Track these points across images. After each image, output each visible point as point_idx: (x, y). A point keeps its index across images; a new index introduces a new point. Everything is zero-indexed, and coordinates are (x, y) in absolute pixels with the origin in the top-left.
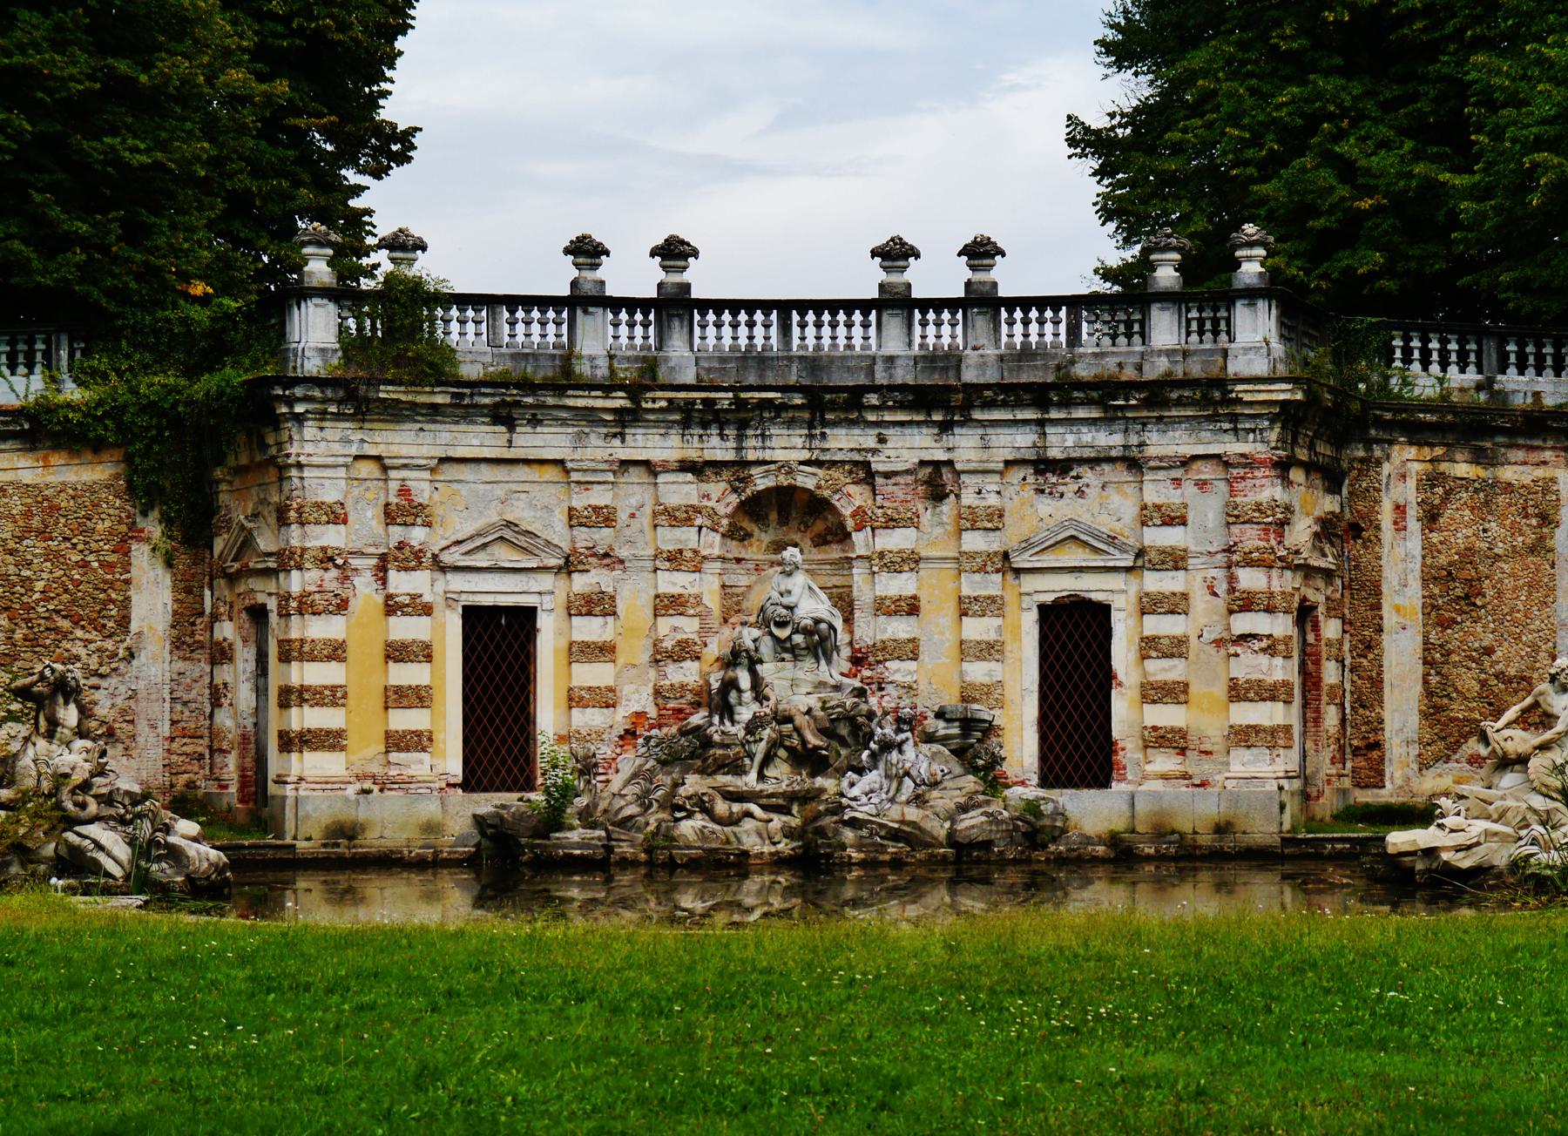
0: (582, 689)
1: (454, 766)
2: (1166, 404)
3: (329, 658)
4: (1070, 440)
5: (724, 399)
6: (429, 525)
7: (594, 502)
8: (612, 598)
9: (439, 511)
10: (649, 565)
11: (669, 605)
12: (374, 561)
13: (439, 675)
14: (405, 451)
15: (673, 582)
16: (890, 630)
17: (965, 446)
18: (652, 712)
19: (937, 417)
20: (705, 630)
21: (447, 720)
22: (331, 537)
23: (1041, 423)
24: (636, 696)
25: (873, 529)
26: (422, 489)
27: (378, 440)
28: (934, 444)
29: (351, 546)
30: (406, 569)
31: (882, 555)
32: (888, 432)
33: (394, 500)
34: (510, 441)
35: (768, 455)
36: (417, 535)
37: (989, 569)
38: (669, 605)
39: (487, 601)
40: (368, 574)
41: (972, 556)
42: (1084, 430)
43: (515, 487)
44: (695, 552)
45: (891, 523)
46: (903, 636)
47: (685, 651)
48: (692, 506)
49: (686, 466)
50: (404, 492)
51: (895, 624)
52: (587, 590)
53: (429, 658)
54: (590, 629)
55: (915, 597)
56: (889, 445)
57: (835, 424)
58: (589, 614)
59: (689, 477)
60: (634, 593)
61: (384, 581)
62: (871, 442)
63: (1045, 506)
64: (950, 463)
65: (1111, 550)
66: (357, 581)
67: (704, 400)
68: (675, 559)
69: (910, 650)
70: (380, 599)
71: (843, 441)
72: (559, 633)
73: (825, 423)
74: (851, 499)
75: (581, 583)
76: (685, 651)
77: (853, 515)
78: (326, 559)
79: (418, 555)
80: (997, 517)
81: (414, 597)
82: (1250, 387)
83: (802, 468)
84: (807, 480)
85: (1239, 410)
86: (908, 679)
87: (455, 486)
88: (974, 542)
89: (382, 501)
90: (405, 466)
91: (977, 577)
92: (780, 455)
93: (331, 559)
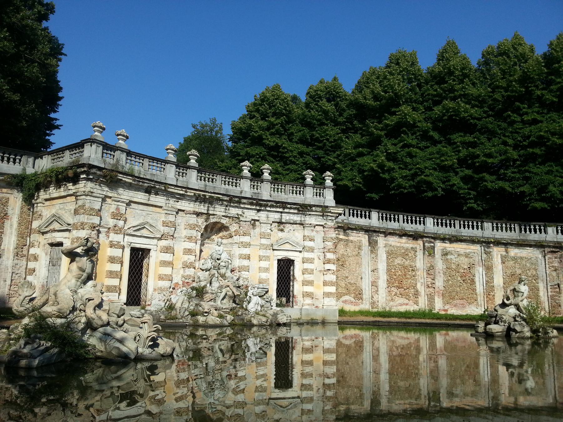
17: (262, 216)
18: (181, 283)
30: (117, 233)
36: (121, 223)
39: (138, 246)
41: (263, 245)
42: (291, 215)
45: (244, 234)
46: (246, 265)
50: (118, 209)
52: (166, 245)
59: (195, 216)
62: (240, 213)
63: (280, 234)
64: (258, 221)
68: (190, 238)
69: (247, 269)
70: (107, 242)
71: (234, 211)
73: (230, 206)
74: (234, 228)
77: (235, 231)
84: (224, 221)
85: (329, 214)
88: (264, 241)
92: (218, 213)
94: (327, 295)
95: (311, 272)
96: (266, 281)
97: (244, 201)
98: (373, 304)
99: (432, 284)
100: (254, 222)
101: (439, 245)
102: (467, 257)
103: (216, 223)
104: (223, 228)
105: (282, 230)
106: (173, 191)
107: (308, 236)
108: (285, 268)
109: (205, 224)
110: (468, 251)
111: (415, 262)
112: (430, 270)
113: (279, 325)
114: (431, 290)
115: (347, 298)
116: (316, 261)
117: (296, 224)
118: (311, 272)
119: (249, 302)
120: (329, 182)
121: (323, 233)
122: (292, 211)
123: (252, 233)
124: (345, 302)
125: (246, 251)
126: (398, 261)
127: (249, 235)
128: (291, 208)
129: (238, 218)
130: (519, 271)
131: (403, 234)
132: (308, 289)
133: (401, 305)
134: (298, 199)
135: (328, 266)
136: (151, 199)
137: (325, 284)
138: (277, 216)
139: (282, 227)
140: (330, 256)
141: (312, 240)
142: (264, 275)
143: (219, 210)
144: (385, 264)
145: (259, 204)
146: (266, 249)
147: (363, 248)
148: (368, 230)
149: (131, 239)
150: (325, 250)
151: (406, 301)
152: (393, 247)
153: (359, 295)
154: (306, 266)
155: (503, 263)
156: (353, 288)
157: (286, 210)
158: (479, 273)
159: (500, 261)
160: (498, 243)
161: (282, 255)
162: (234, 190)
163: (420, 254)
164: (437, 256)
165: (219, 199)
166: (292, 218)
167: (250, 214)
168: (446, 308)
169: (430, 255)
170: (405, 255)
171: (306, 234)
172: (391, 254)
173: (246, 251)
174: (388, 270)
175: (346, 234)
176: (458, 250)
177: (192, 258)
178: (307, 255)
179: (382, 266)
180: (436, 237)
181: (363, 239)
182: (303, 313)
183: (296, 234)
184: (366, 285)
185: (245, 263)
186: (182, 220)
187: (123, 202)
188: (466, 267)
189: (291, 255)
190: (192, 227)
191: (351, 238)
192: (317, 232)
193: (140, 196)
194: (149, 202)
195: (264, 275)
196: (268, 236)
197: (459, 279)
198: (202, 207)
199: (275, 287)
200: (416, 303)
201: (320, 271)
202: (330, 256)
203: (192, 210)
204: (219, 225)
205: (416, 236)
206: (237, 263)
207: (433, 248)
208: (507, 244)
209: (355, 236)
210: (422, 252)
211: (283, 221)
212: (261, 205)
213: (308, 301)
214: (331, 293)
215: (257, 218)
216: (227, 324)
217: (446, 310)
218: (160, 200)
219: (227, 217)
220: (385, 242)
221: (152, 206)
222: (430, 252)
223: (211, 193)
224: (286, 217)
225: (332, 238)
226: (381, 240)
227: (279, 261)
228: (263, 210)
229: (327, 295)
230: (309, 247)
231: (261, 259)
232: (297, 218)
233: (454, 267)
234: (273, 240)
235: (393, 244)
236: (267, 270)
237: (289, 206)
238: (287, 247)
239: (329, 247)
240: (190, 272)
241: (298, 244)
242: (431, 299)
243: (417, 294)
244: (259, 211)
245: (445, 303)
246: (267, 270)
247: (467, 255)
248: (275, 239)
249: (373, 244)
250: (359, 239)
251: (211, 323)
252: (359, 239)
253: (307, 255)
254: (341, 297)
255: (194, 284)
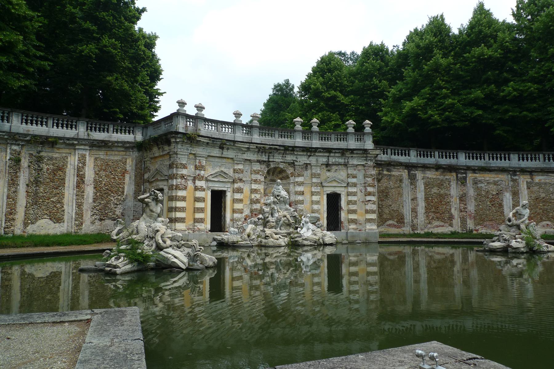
1: (209, 227)
3: (183, 200)
4: (334, 160)
5: (267, 147)
6: (204, 170)
9: (207, 167)
11: (253, 191)
13: (206, 205)
15: (254, 186)
17: (313, 160)
18: (250, 214)
19: (309, 154)
20: (261, 197)
22: (184, 172)
23: (328, 156)
26: (204, 163)
29: (189, 174)
31: (297, 182)
39: (216, 189)
41: (315, 183)
45: (299, 175)
47: (257, 201)
49: (258, 161)
50: (200, 162)
53: (204, 201)
54: (238, 196)
57: (288, 154)
59: (258, 164)
60: (246, 188)
61: (194, 183)
62: (295, 159)
63: (328, 174)
64: (310, 164)
66: (188, 182)
68: (256, 181)
69: (302, 202)
71: (290, 158)
72: (231, 197)
73: (286, 154)
74: (290, 170)
75: (236, 186)
76: (257, 201)
78: (182, 177)
80: (319, 175)
81: (201, 187)
84: (281, 166)
88: (314, 180)
90: (200, 157)
92: (277, 160)
94: (369, 221)
95: (355, 203)
96: (317, 211)
97: (298, 149)
98: (414, 227)
99: (464, 208)
100: (306, 166)
101: (470, 176)
102: (495, 184)
103: (275, 168)
104: (282, 171)
105: (329, 171)
106: (240, 146)
107: (351, 174)
108: (334, 200)
109: (267, 169)
110: (496, 179)
111: (449, 190)
112: (463, 198)
113: (325, 245)
114: (464, 213)
115: (390, 222)
116: (359, 194)
117: (341, 165)
118: (355, 203)
119: (302, 228)
120: (368, 129)
121: (363, 171)
122: (337, 155)
123: (305, 175)
124: (390, 225)
125: (300, 189)
126: (435, 190)
127: (303, 175)
128: (335, 153)
129: (293, 163)
130: (543, 195)
131: (438, 167)
132: (352, 216)
133: (437, 227)
134: (342, 145)
135: (368, 198)
136: (224, 153)
137: (367, 212)
138: (324, 160)
139: (329, 168)
140: (370, 189)
141: (355, 177)
142: (316, 207)
143: (277, 158)
144: (423, 194)
145: (310, 151)
146: (316, 186)
147: (404, 181)
148: (409, 167)
149: (210, 184)
150: (366, 185)
151: (442, 224)
152: (430, 179)
153: (401, 221)
154: (350, 198)
155: (528, 188)
156: (396, 214)
157: (332, 155)
158: (507, 198)
159: (525, 187)
160: (523, 171)
161: (330, 190)
162: (288, 142)
163: (453, 184)
164: (468, 185)
165: (276, 149)
166: (337, 160)
167: (303, 159)
168: (477, 228)
169: (462, 183)
170: (440, 185)
171: (350, 172)
172: (426, 185)
173: (300, 189)
174: (426, 199)
175: (388, 170)
176: (487, 179)
177: (258, 196)
178: (351, 189)
179: (421, 195)
180: (468, 168)
181: (403, 173)
182: (349, 235)
183: (342, 173)
184: (407, 212)
185: (300, 198)
186: (247, 167)
187: (203, 157)
188: (494, 193)
189: (338, 190)
190: (257, 172)
191: (393, 173)
192: (359, 170)
193: (216, 152)
194: (223, 156)
195: (316, 207)
196: (318, 176)
197: (488, 203)
198: (264, 156)
199: (325, 215)
200: (451, 225)
201: (363, 202)
202: (370, 189)
203: (256, 159)
204: (279, 170)
205: (451, 169)
206: (293, 198)
207: (465, 178)
208: (531, 172)
209: (395, 173)
210: (455, 182)
211: (330, 163)
212: (311, 152)
213: (353, 226)
214: (372, 219)
215: (308, 162)
216: (283, 244)
217: (477, 230)
218: (230, 154)
219: (284, 162)
220: (422, 175)
221: (225, 158)
222: (463, 182)
223: (270, 145)
224: (332, 160)
225: (371, 175)
226: (419, 175)
227: (328, 195)
228: (313, 156)
229: (369, 221)
230: (352, 183)
231: (312, 194)
232: (341, 161)
233: (483, 193)
234: (323, 177)
235: (430, 176)
236: (318, 203)
237: (334, 151)
238: (335, 184)
239: (369, 182)
240: (257, 206)
241: (342, 181)
242: (463, 221)
243: (451, 217)
244: (310, 156)
245: (476, 225)
246: (318, 203)
247: (495, 183)
248: (325, 177)
249: (413, 178)
250: (399, 173)
251: (271, 244)
252: (399, 173)
253: (351, 189)
254: (386, 221)
255: (261, 216)
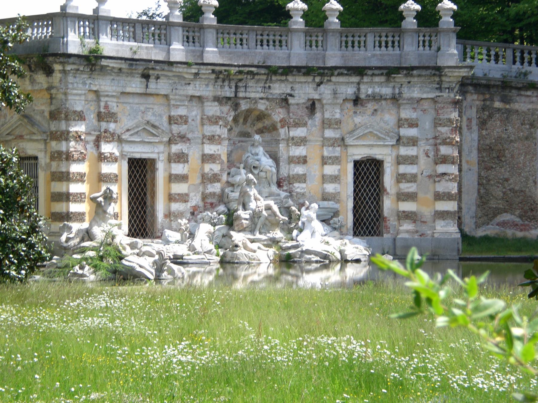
0: (175, 194)
2: (412, 76)
6: (116, 122)
7: (180, 113)
8: (187, 155)
9: (119, 115)
10: (200, 141)
11: (206, 158)
12: (94, 138)
14: (107, 88)
15: (210, 149)
16: (296, 170)
18: (201, 204)
20: (222, 170)
21: (121, 207)
24: (195, 198)
25: (288, 128)
26: (114, 106)
27: (97, 83)
28: (314, 92)
31: (293, 139)
32: (297, 86)
33: (102, 110)
34: (147, 86)
35: (248, 95)
36: (112, 126)
37: (335, 145)
38: (206, 158)
39: (138, 156)
40: (92, 143)
41: (329, 139)
43: (148, 106)
44: (219, 136)
45: (297, 125)
46: (301, 173)
47: (215, 178)
48: (218, 116)
50: (106, 107)
51: (298, 168)
52: (177, 152)
54: (178, 169)
55: (306, 157)
56: (296, 92)
58: (179, 162)
59: (216, 103)
60: (194, 153)
62: (289, 91)
65: (387, 138)
67: (225, 71)
68: (212, 139)
69: (302, 178)
70: (96, 155)
71: (279, 88)
72: (165, 170)
75: (175, 148)
76: (215, 178)
77: (281, 121)
79: (113, 135)
80: (339, 122)
82: (451, 70)
83: (260, 101)
84: (262, 106)
86: (302, 191)
87: (125, 105)
88: (329, 133)
89: (96, 111)
90: (107, 96)
91: (330, 148)
92: (252, 95)
93: (80, 137)
167: (304, 90)
